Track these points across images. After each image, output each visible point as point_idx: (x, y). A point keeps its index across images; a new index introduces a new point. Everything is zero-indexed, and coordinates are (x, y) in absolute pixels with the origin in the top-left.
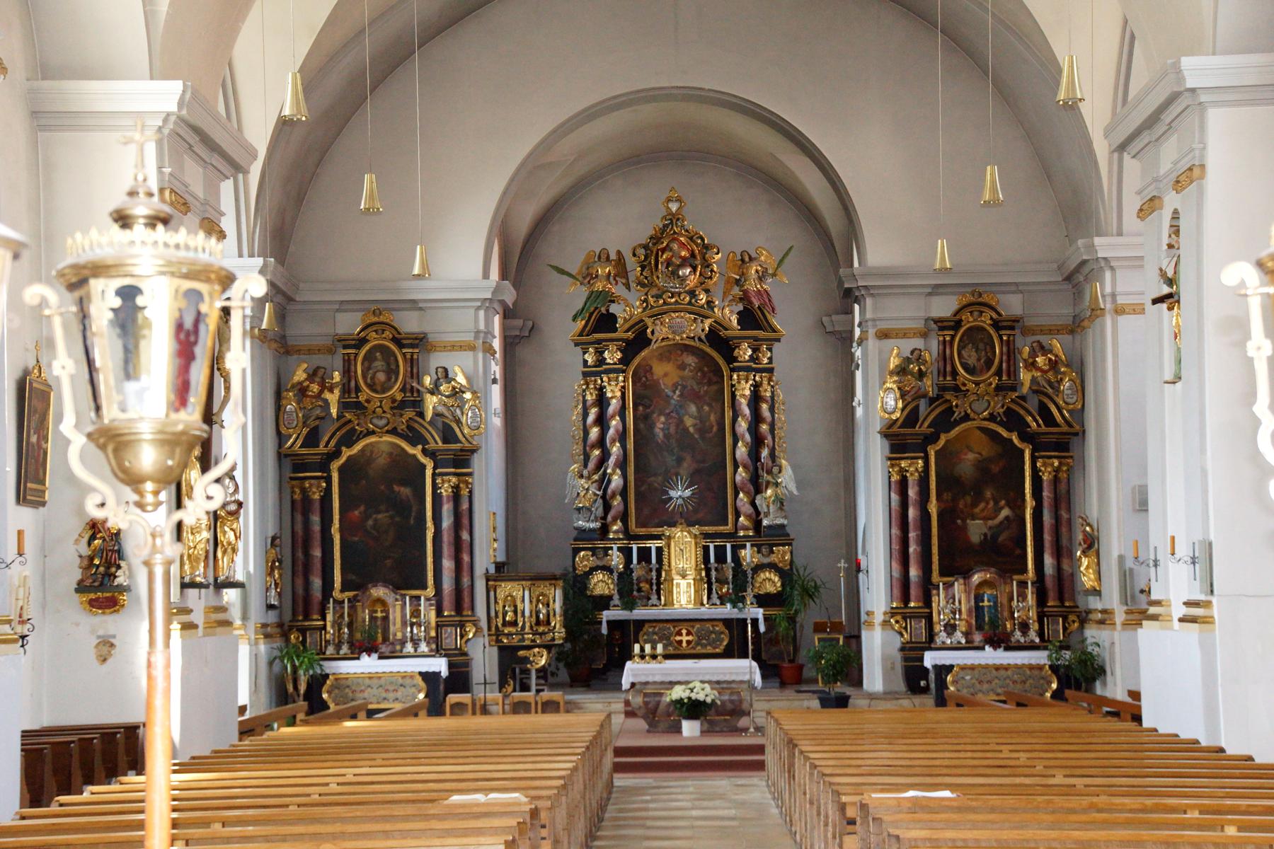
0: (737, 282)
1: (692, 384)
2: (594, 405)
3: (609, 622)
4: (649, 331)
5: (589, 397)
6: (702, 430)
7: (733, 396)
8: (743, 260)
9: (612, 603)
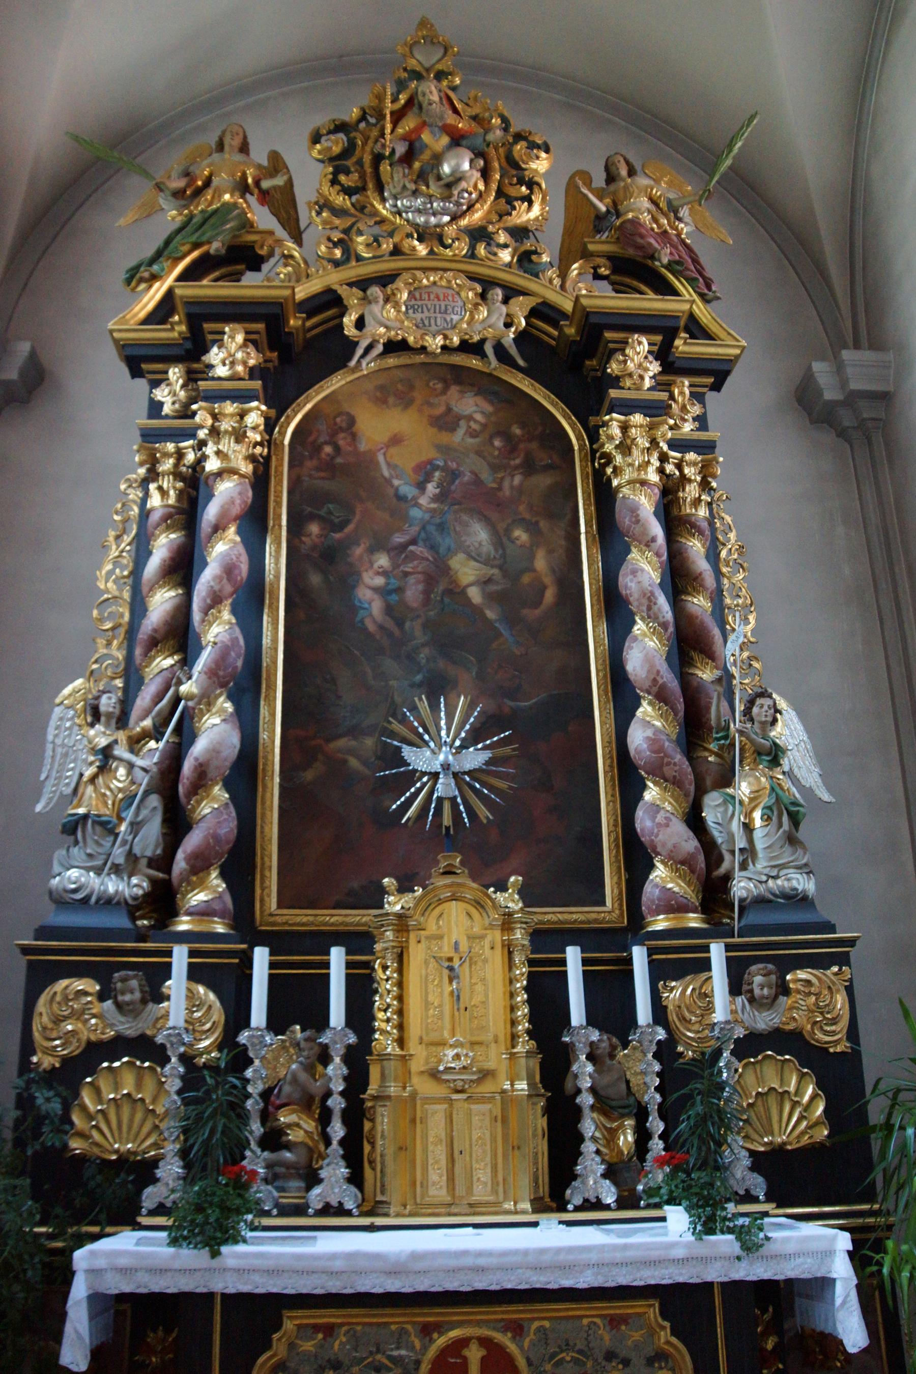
0: (599, 222)
1: (475, 467)
2: (169, 520)
3: (99, 1302)
4: (349, 320)
5: (155, 500)
6: (511, 594)
7: (605, 497)
8: (611, 178)
9: (151, 1196)
